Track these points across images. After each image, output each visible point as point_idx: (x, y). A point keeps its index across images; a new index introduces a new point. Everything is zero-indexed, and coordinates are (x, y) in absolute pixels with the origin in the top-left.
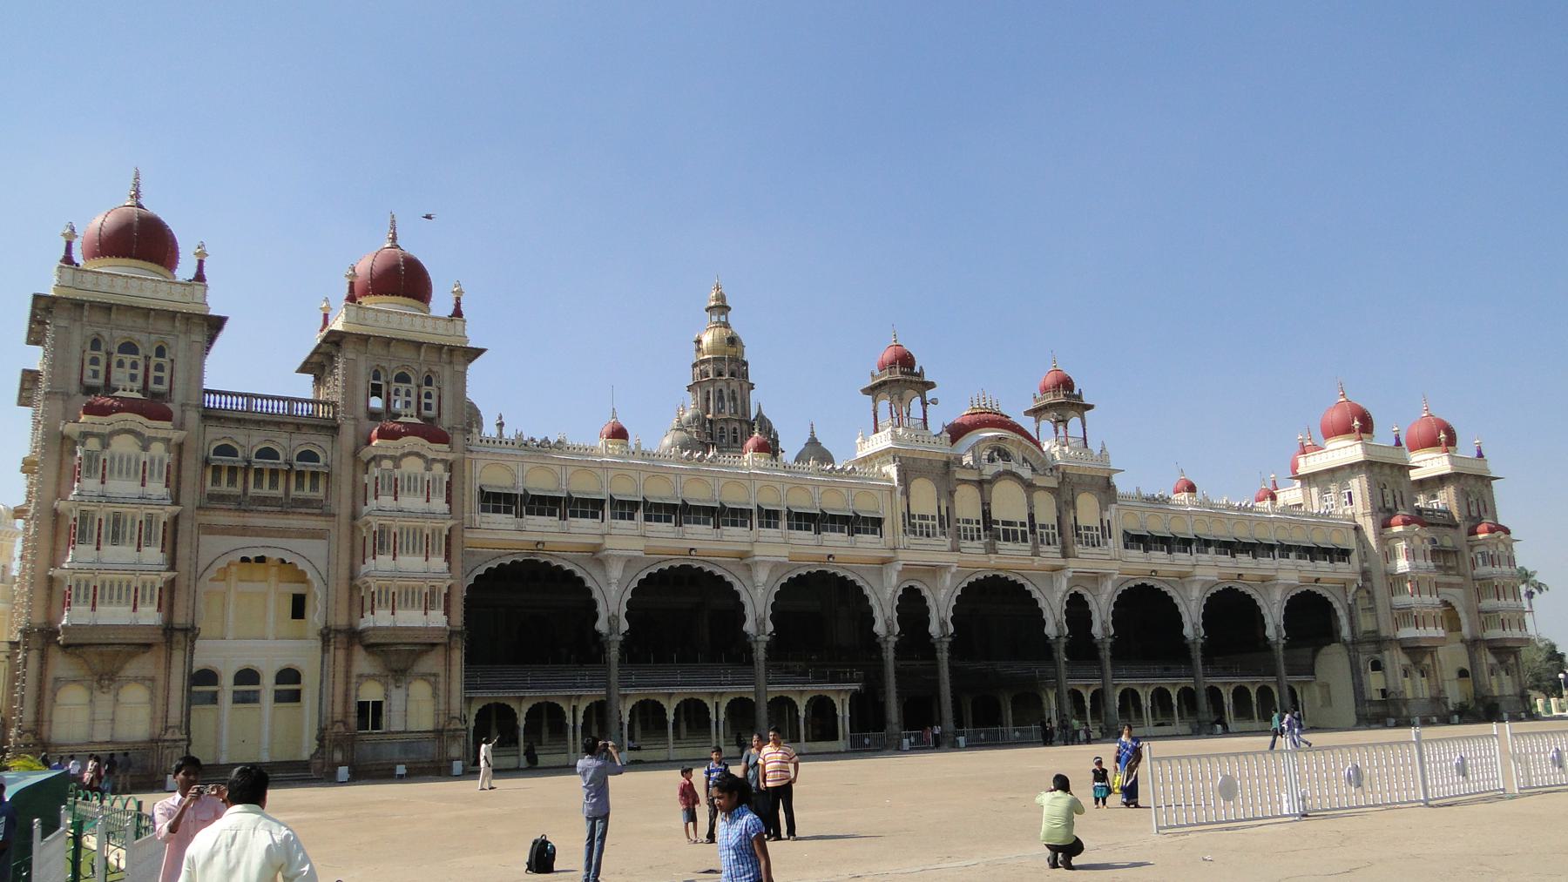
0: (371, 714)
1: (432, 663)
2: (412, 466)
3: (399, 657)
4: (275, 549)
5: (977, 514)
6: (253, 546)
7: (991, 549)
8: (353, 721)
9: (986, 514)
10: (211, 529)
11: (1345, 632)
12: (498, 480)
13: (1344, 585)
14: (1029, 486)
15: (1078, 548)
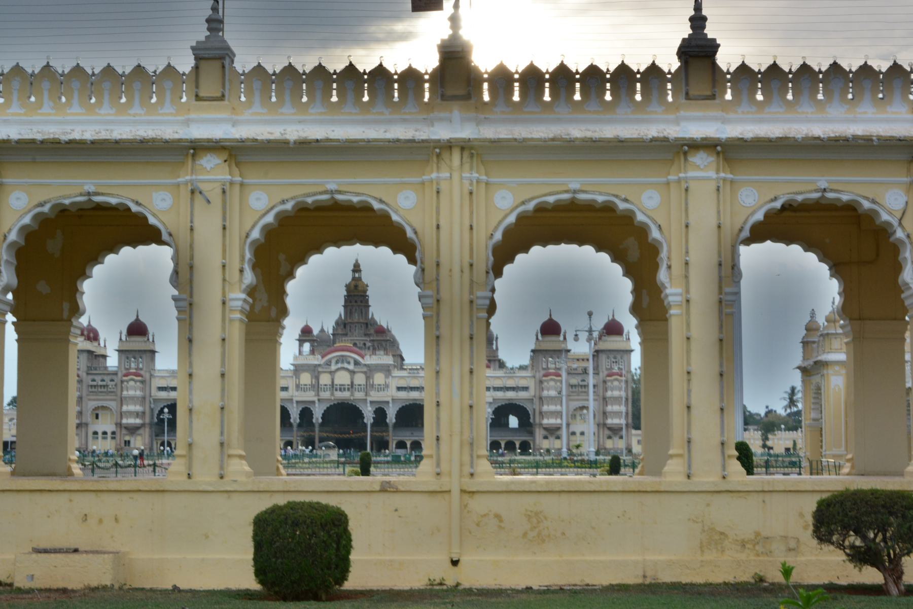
0: (127, 443)
1: (141, 431)
2: (132, 383)
3: (133, 430)
4: (105, 404)
5: (329, 382)
6: (100, 403)
7: (332, 394)
8: (123, 445)
9: (333, 382)
10: (90, 400)
11: (531, 421)
12: (163, 383)
13: (531, 400)
14: (352, 373)
15: (372, 393)
